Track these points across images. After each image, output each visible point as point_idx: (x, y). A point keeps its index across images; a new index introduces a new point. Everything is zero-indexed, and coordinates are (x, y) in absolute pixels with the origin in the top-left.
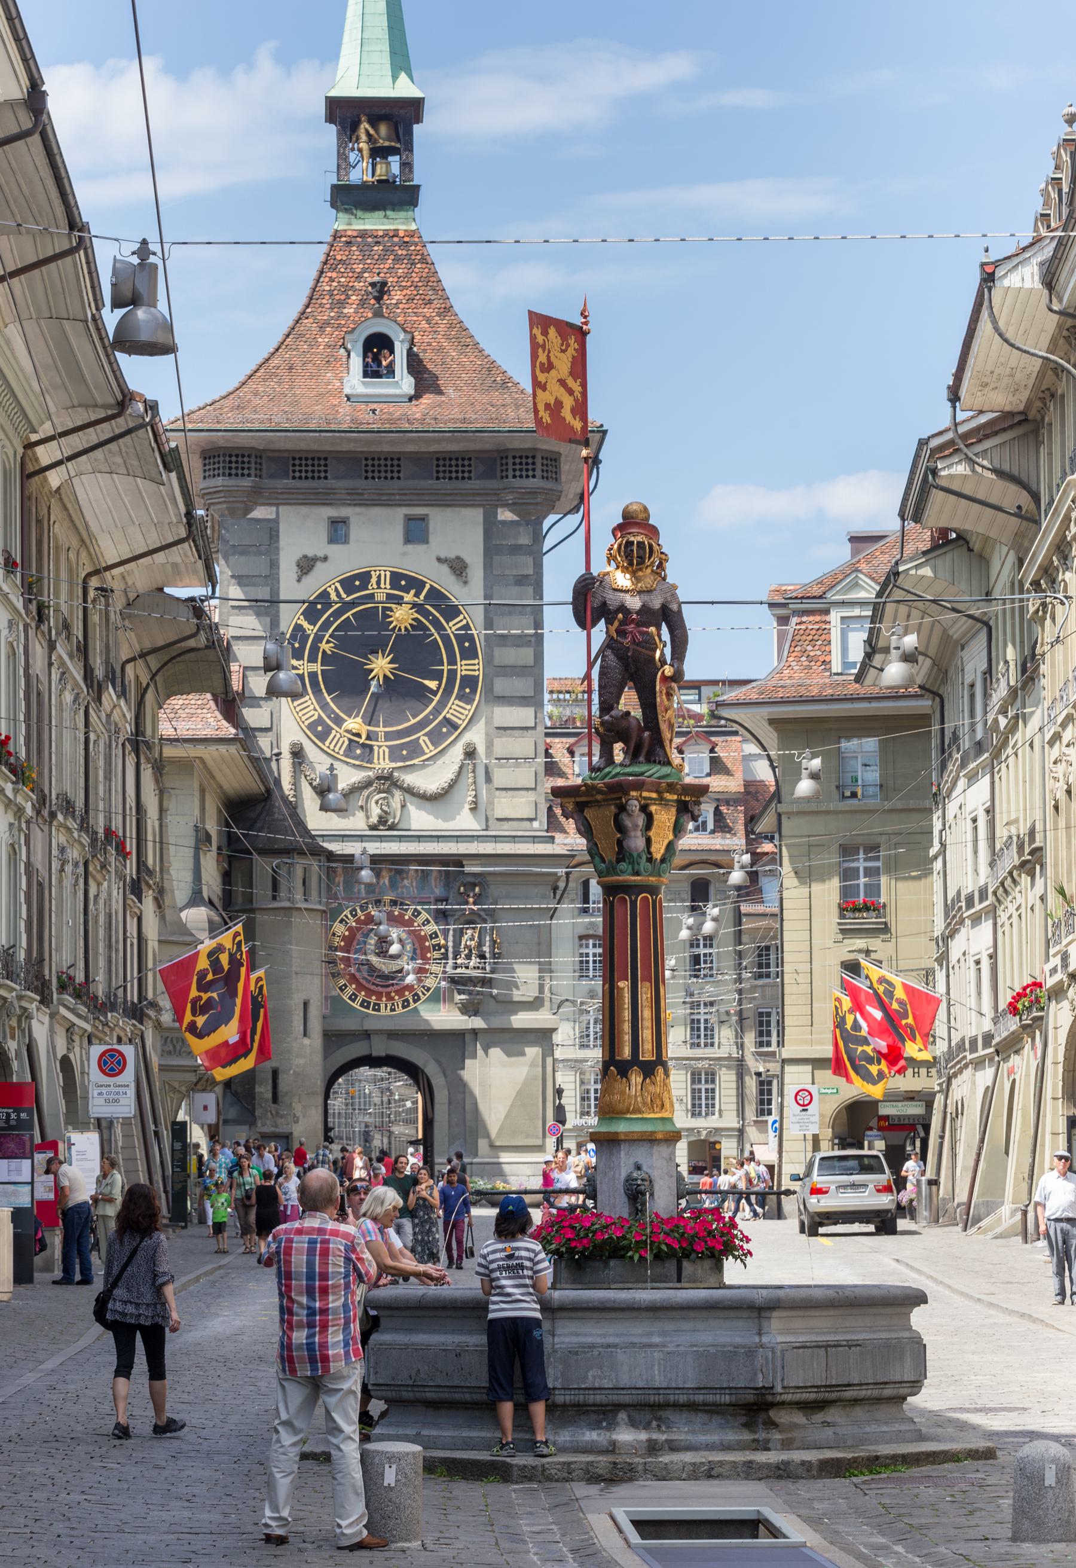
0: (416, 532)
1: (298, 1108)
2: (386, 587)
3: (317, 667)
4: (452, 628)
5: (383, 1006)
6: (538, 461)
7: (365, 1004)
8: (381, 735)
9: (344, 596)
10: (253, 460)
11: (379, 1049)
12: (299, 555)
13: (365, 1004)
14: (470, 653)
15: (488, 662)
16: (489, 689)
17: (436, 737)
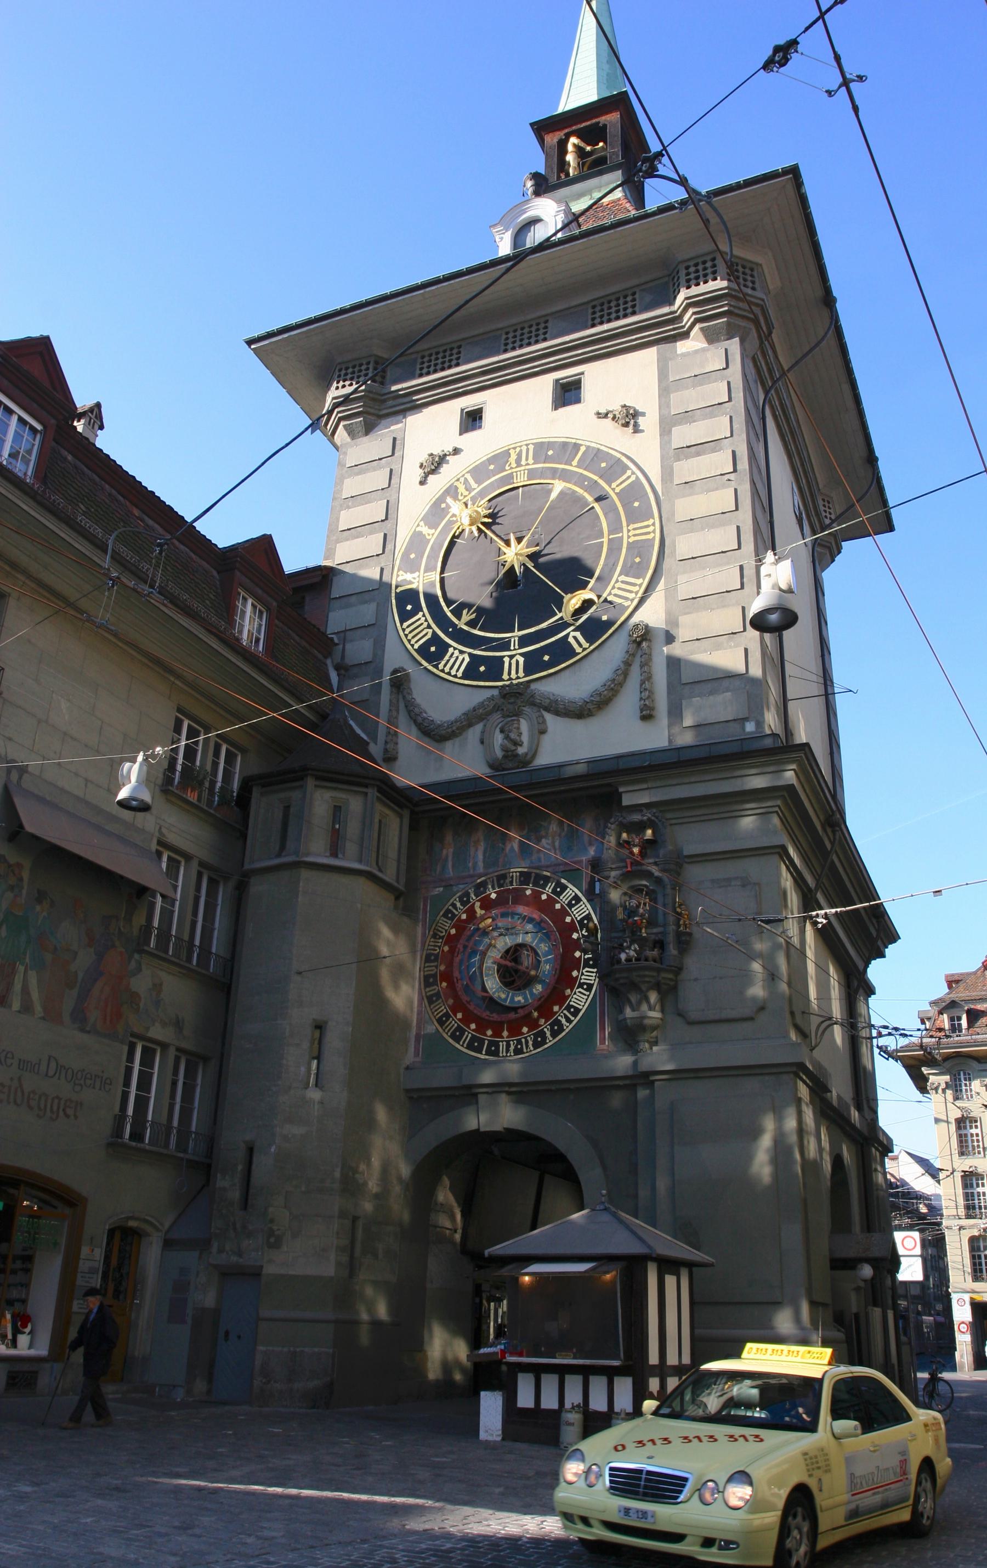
2: (530, 463)
5: (502, 1046)
6: (720, 263)
7: (476, 1045)
8: (514, 643)
9: (474, 485)
10: (371, 366)
12: (423, 458)
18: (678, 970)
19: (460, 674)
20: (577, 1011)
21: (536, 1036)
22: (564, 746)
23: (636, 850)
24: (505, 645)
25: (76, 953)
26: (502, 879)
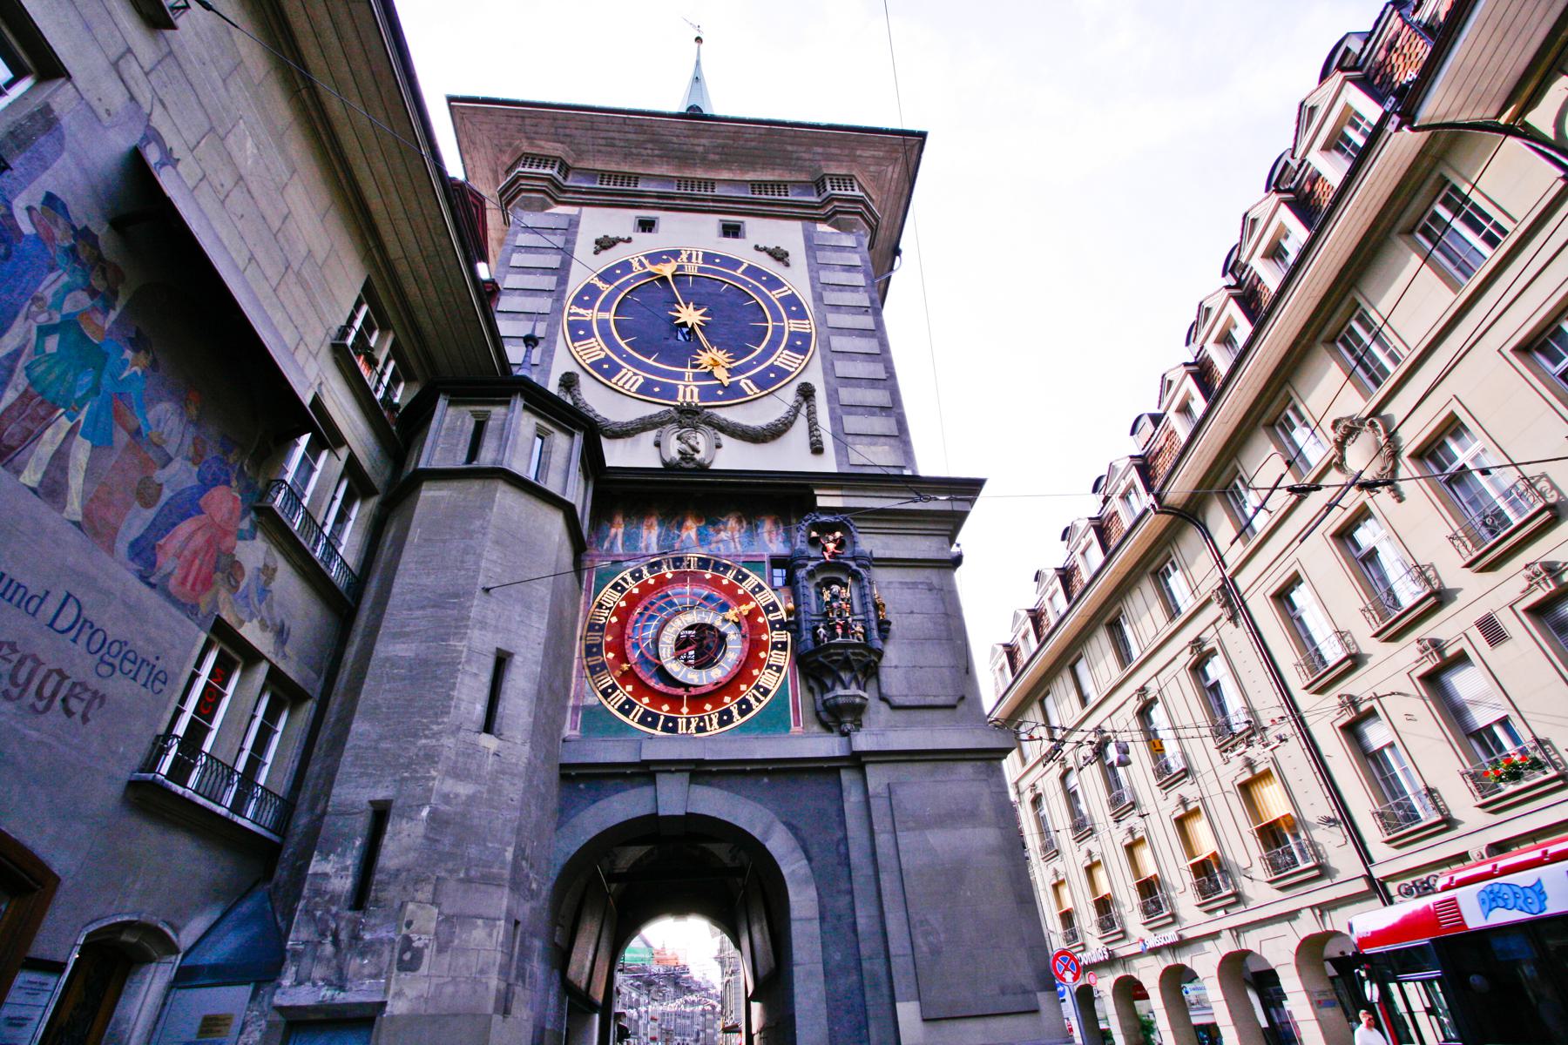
1: (424, 921)
4: (775, 295)
7: (648, 719)
11: (673, 798)
12: (600, 236)
13: (648, 719)
15: (821, 322)
17: (763, 382)
18: (880, 654)
19: (634, 389)
20: (766, 692)
21: (721, 714)
23: (831, 546)
24: (681, 376)
25: (170, 459)
26: (678, 561)
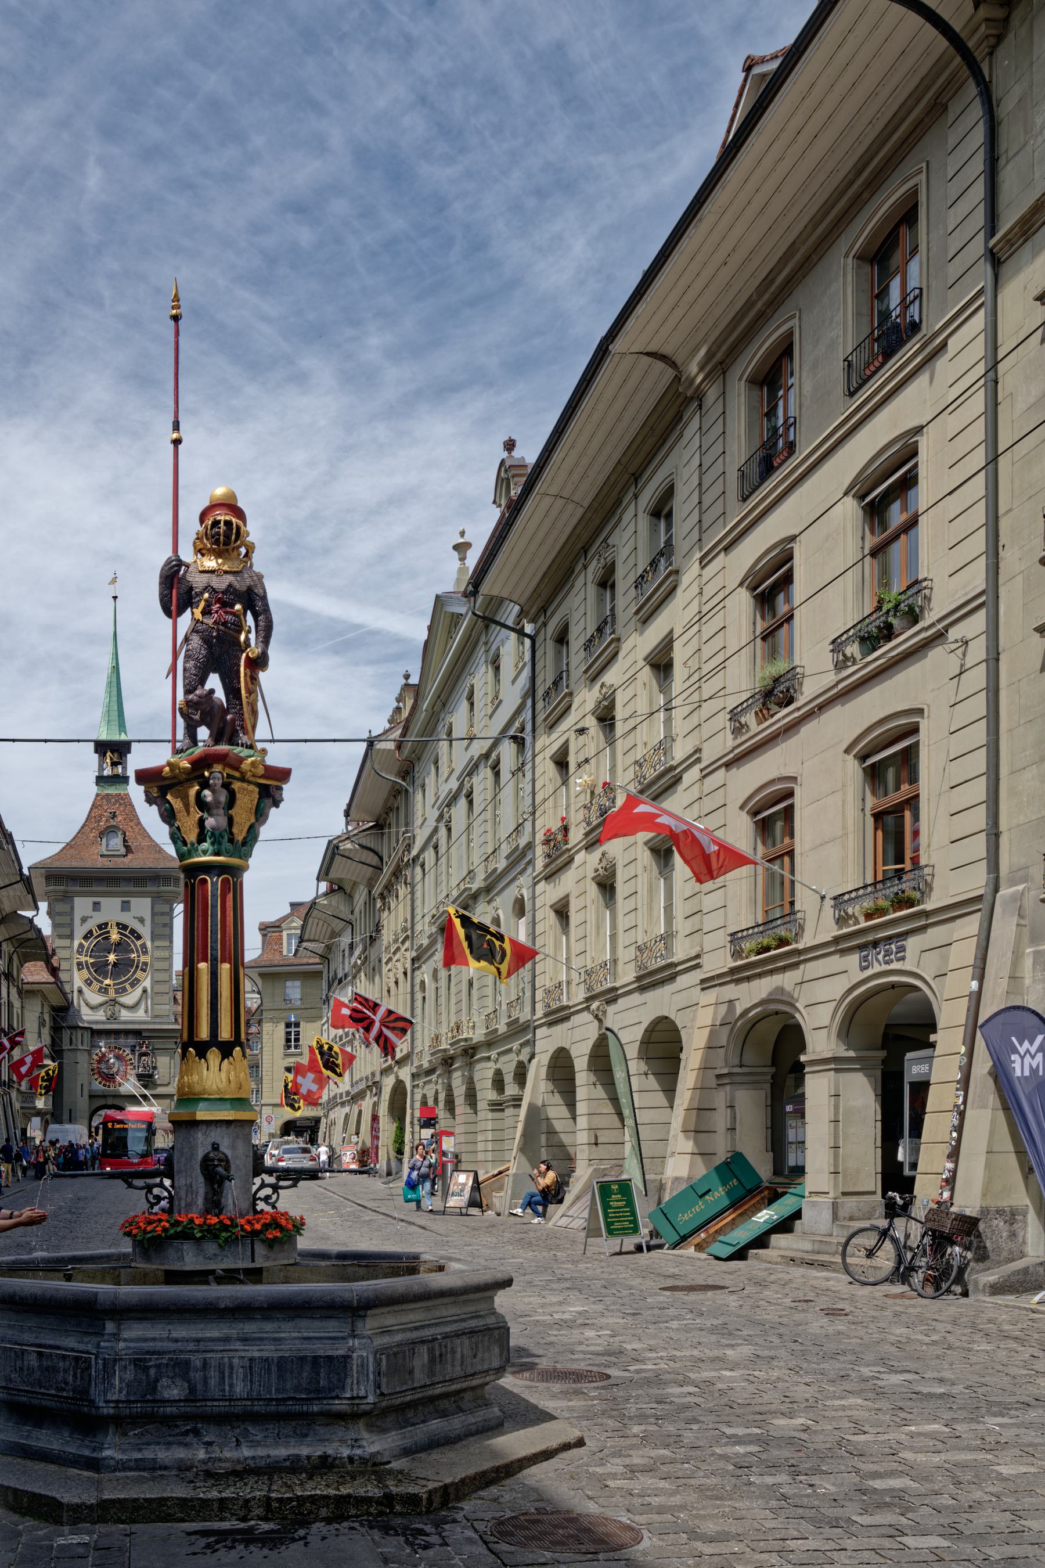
0: (126, 907)
3: (88, 958)
4: (139, 943)
7: (104, 1085)
14: (145, 953)
15: (152, 956)
16: (152, 966)
22: (125, 1015)
